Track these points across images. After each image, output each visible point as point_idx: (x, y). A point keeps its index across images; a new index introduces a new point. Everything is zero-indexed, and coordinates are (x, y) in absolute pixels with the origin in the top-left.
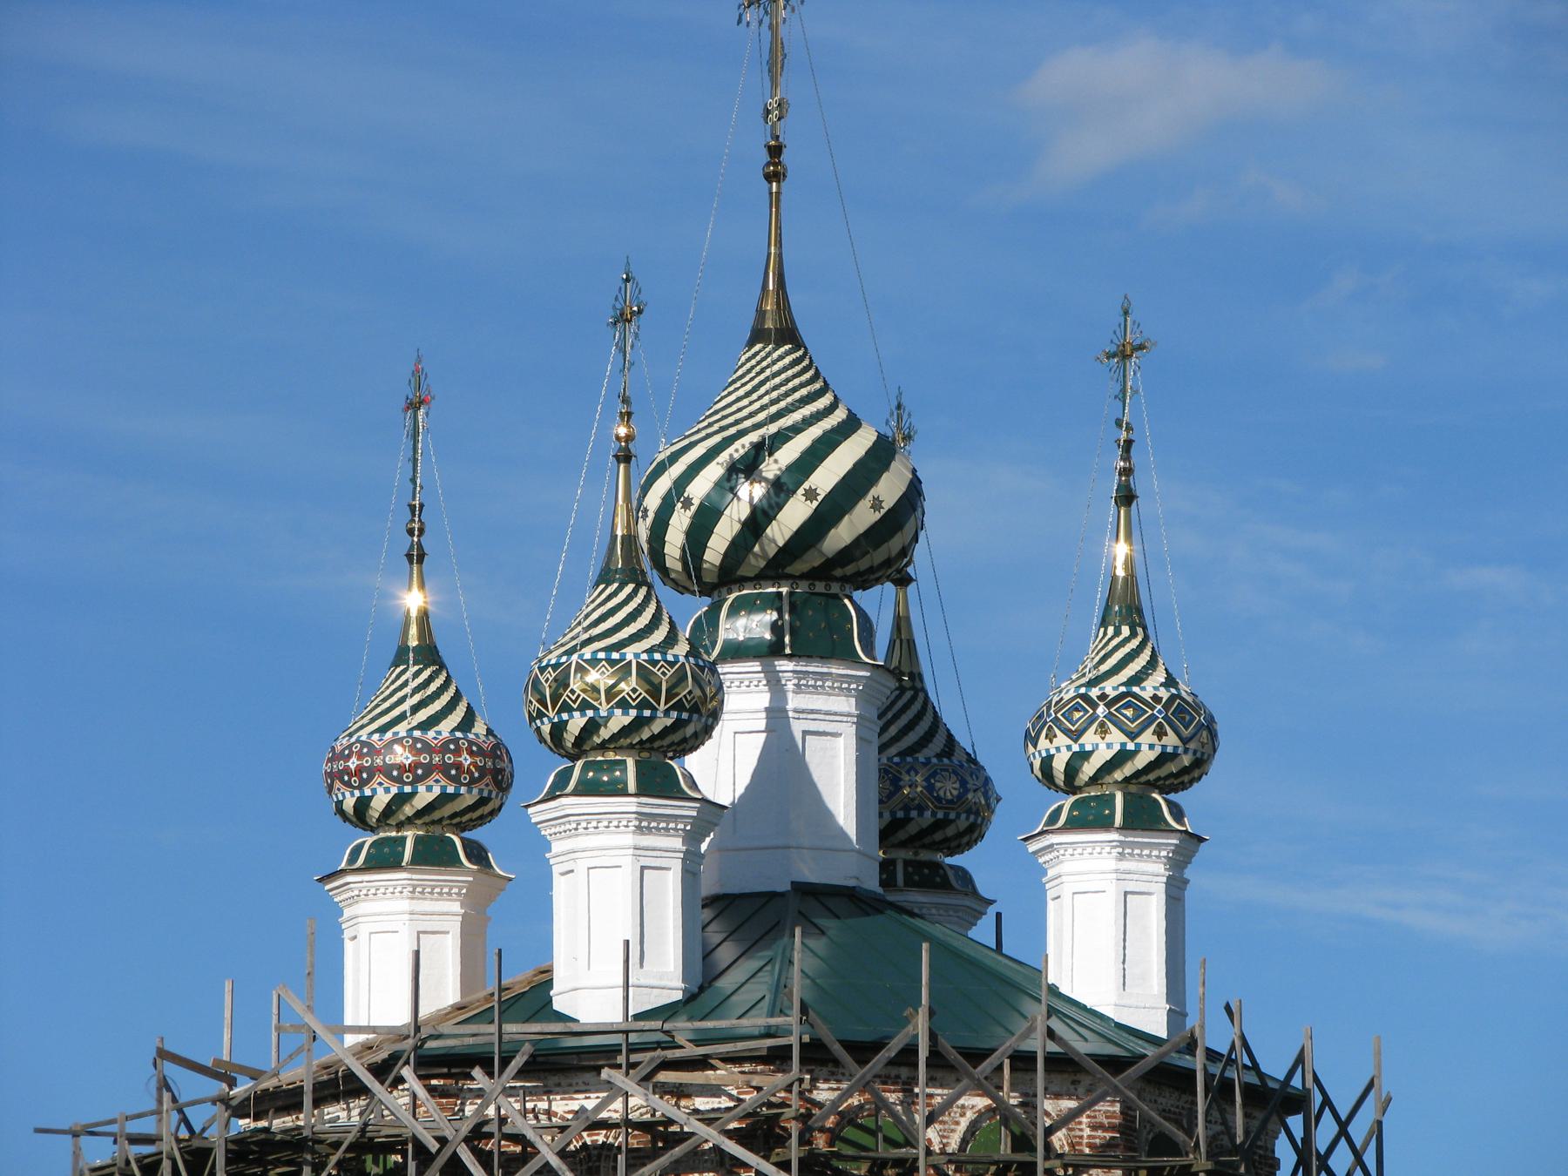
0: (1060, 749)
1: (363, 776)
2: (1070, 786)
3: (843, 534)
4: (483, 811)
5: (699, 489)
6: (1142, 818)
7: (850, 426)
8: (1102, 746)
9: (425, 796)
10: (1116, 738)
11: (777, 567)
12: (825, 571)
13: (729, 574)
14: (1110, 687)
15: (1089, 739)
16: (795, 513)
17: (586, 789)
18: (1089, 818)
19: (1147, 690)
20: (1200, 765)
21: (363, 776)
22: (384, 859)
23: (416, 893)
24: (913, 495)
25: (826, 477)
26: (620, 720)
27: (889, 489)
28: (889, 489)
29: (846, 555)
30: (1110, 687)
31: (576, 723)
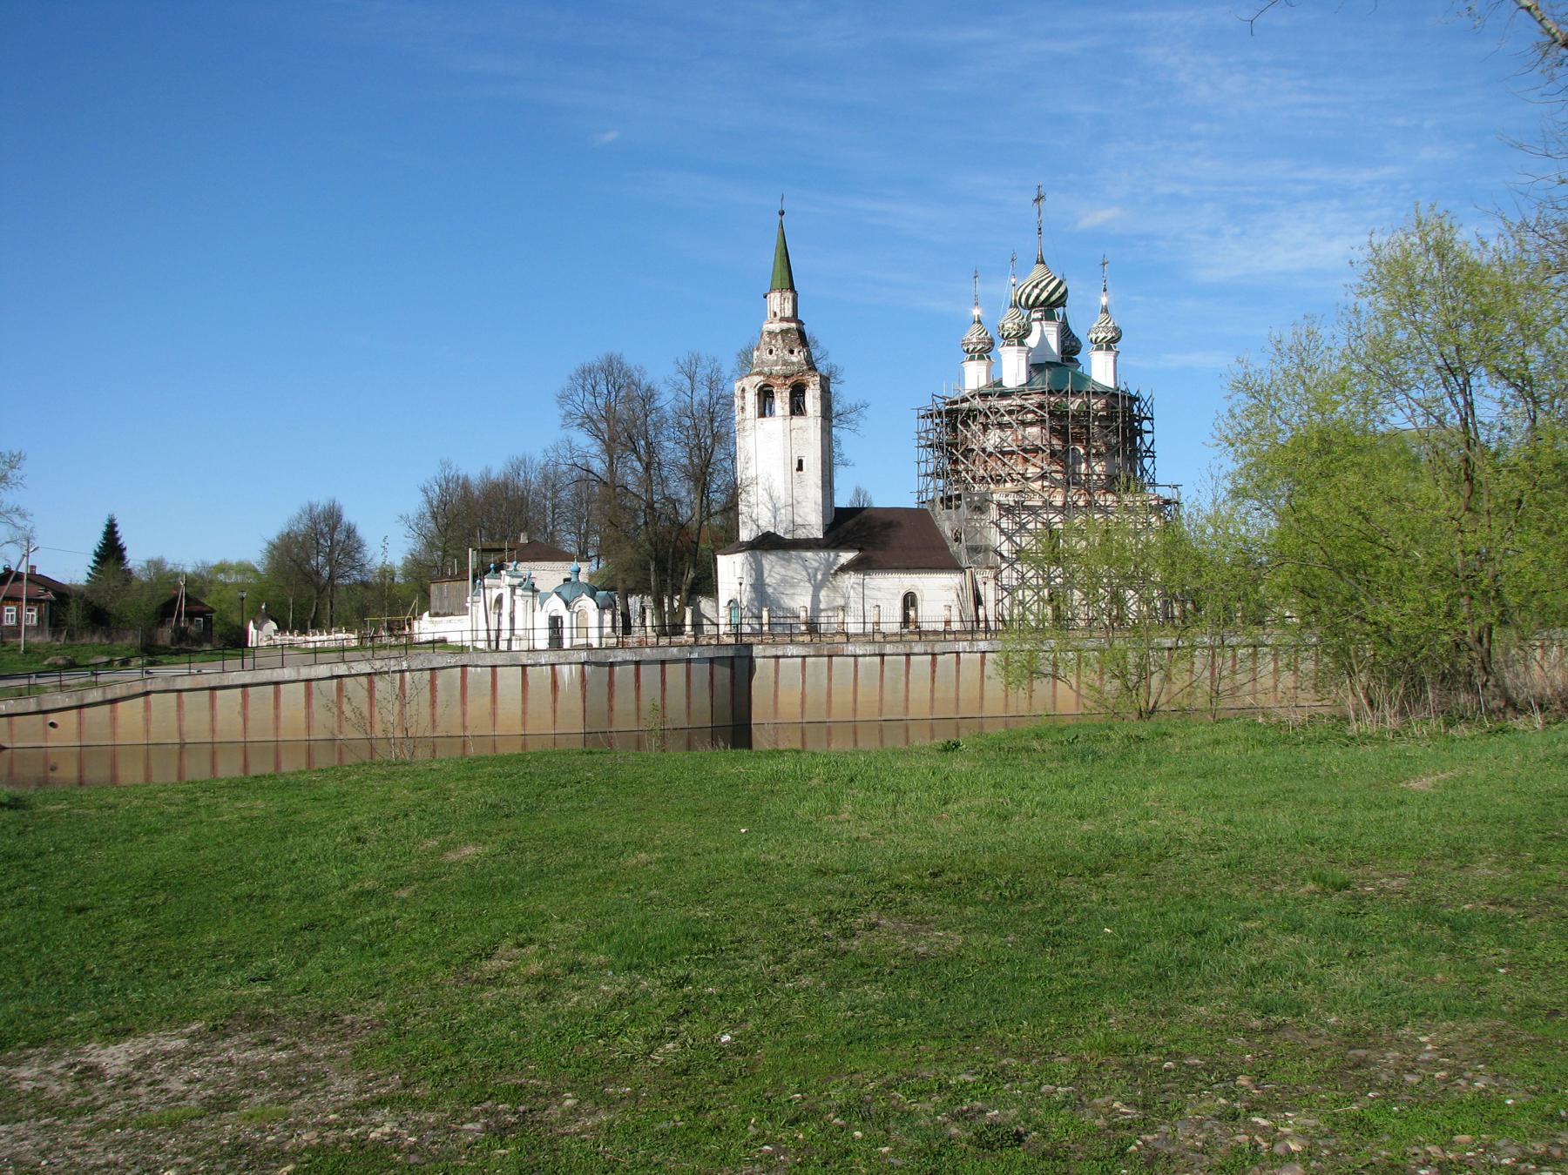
0: (1094, 336)
1: (969, 344)
2: (1096, 342)
3: (1053, 298)
4: (989, 350)
5: (1027, 291)
6: (1109, 348)
7: (1055, 278)
8: (1101, 336)
9: (979, 348)
10: (1104, 334)
11: (1042, 304)
12: (1051, 305)
13: (1033, 306)
14: (1103, 325)
15: (1099, 334)
16: (1045, 295)
17: (1008, 345)
18: (1099, 348)
19: (1109, 325)
20: (1119, 339)
21: (969, 344)
22: (972, 359)
23: (978, 365)
24: (1066, 290)
25: (1050, 288)
26: (1014, 333)
27: (1062, 290)
28: (1062, 290)
29: (1054, 302)
30: (1103, 325)
31: (1006, 334)
